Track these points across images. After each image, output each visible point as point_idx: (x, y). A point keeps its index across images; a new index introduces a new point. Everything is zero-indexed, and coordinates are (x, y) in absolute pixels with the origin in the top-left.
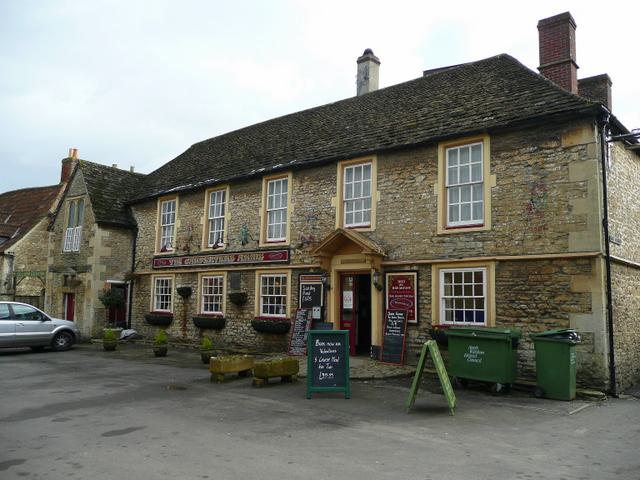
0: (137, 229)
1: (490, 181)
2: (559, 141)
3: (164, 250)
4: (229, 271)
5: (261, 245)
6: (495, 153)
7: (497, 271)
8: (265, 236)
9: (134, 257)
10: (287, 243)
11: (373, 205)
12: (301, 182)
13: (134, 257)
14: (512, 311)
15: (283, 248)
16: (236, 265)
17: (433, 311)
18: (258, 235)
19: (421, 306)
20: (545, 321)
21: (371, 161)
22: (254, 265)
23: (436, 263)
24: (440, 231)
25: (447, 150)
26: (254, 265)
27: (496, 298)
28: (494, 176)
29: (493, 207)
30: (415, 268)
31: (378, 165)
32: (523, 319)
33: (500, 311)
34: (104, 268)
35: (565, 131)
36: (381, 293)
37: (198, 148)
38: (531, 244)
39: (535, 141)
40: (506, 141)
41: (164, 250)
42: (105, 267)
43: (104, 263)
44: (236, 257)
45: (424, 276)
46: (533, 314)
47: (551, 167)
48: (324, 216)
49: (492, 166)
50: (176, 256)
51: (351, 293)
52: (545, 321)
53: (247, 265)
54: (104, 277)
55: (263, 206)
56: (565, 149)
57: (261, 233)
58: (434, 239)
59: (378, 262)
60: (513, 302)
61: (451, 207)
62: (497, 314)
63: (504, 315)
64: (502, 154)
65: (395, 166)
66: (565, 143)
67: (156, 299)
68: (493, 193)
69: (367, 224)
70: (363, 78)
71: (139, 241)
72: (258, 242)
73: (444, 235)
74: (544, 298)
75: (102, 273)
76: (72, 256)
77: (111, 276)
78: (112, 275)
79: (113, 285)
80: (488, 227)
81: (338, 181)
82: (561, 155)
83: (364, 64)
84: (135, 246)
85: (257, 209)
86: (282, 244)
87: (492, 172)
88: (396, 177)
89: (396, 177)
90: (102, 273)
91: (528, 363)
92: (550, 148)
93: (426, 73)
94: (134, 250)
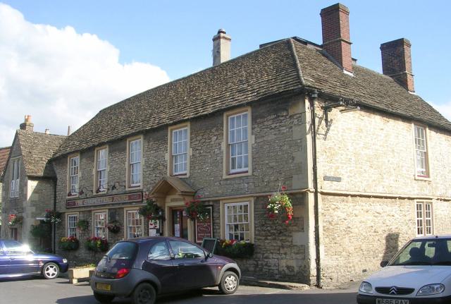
0: (57, 179)
1: (251, 140)
2: (287, 110)
3: (70, 194)
4: (109, 209)
5: (127, 189)
6: (254, 119)
7: (255, 204)
8: (129, 182)
9: (55, 200)
10: (141, 188)
11: (188, 157)
12: (148, 142)
13: (55, 200)
14: (263, 233)
15: (139, 191)
16: (113, 204)
17: (221, 234)
18: (125, 181)
19: (215, 231)
20: (281, 238)
21: (187, 126)
22: (123, 204)
23: (222, 200)
24: (225, 177)
25: (229, 118)
26: (123, 204)
27: (255, 224)
28: (254, 136)
29: (253, 158)
30: (211, 203)
31: (191, 129)
32: (269, 238)
33: (257, 232)
34: (34, 209)
35: (290, 104)
36: (192, 222)
37: (103, 113)
38: (273, 184)
39: (276, 111)
40: (262, 110)
41: (70, 194)
42: (34, 208)
43: (34, 205)
44: (113, 198)
45: (216, 209)
46: (274, 234)
47: (284, 130)
48: (161, 167)
49: (253, 129)
50: (79, 199)
51: (178, 225)
52: (281, 238)
53: (119, 204)
54: (34, 215)
55: (225, 140)
56: (291, 117)
57: (127, 179)
58: (222, 182)
59: (189, 199)
60: (263, 225)
61: (232, 158)
62: (255, 235)
63: (259, 235)
64: (258, 121)
65: (200, 130)
66: (291, 112)
67: (69, 230)
68: (253, 148)
69: (184, 172)
70: (217, 53)
71: (58, 188)
72: (92, 191)
73: (227, 180)
74: (280, 222)
75: (32, 213)
76: (15, 199)
77: (39, 215)
78: (41, 214)
79: (41, 221)
80: (250, 173)
81: (169, 141)
82: (288, 122)
83: (217, 42)
84: (55, 192)
85: (124, 162)
86: (138, 188)
87: (252, 134)
88: (201, 137)
89: (201, 137)
90: (32, 213)
91: (272, 268)
92: (283, 116)
93: (261, 46)
94: (55, 195)
